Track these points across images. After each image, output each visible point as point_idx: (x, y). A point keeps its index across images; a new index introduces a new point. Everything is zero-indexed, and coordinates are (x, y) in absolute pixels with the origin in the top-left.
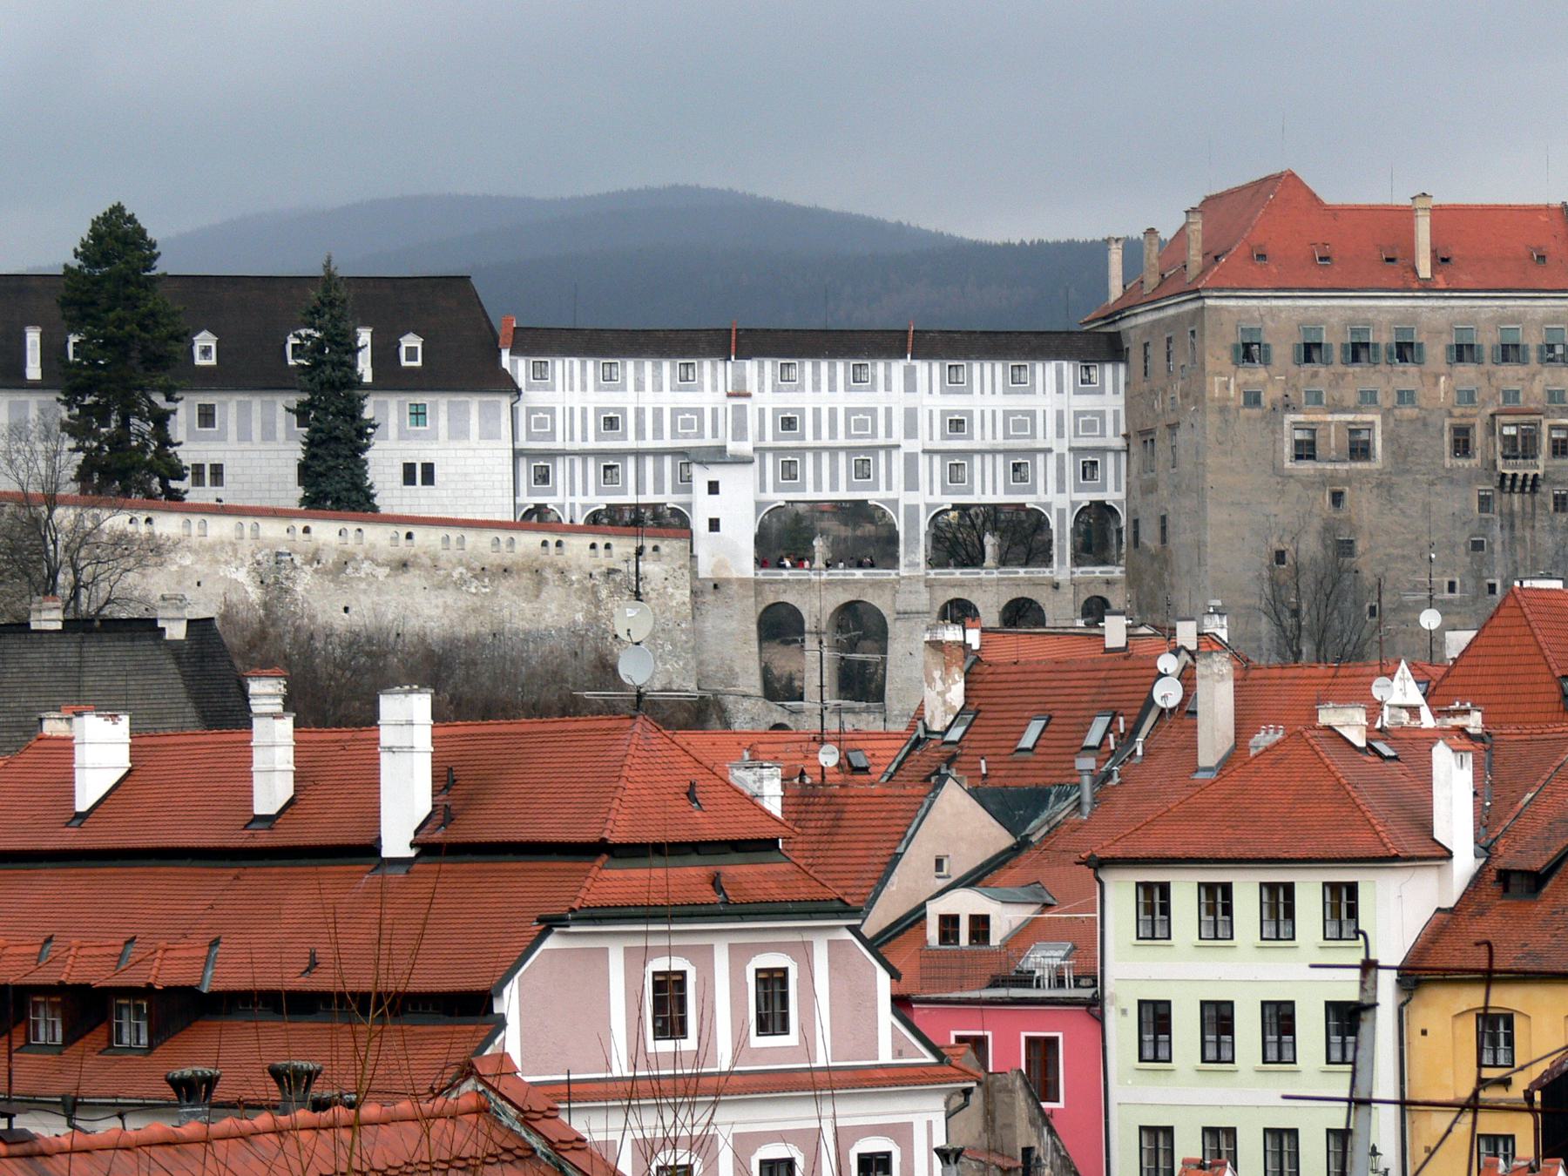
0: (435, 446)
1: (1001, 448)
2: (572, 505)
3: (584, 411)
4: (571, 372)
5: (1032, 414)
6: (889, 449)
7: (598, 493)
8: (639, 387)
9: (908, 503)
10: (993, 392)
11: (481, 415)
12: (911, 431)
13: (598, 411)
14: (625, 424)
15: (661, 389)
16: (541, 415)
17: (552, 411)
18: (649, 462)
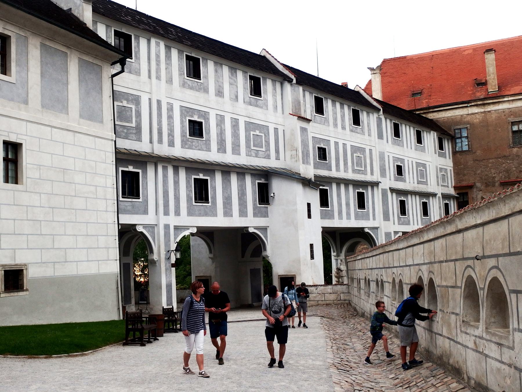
0: (23, 115)
1: (417, 190)
2: (167, 227)
3: (170, 109)
4: (158, 56)
5: (424, 166)
6: (375, 184)
7: (190, 213)
8: (220, 93)
9: (387, 231)
10: (411, 148)
11: (81, 80)
12: (383, 173)
13: (185, 110)
14: (208, 133)
15: (237, 97)
16: (125, 103)
17: (137, 100)
18: (234, 178)
